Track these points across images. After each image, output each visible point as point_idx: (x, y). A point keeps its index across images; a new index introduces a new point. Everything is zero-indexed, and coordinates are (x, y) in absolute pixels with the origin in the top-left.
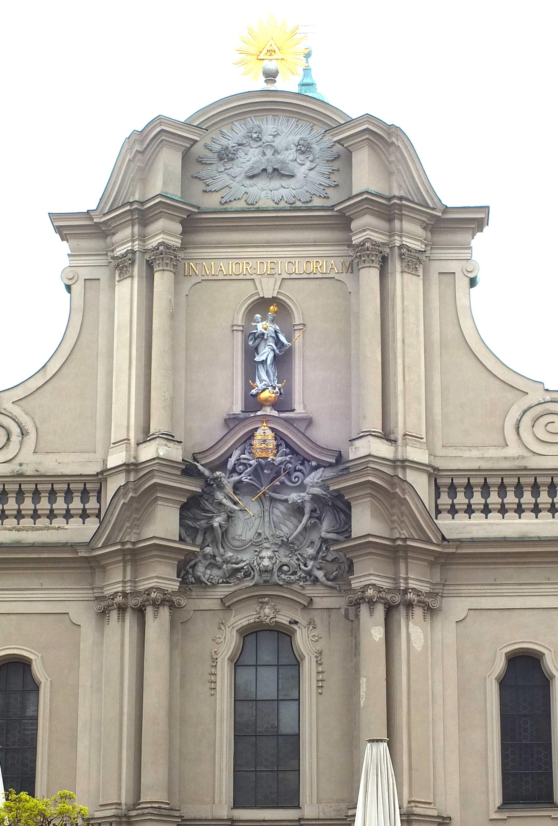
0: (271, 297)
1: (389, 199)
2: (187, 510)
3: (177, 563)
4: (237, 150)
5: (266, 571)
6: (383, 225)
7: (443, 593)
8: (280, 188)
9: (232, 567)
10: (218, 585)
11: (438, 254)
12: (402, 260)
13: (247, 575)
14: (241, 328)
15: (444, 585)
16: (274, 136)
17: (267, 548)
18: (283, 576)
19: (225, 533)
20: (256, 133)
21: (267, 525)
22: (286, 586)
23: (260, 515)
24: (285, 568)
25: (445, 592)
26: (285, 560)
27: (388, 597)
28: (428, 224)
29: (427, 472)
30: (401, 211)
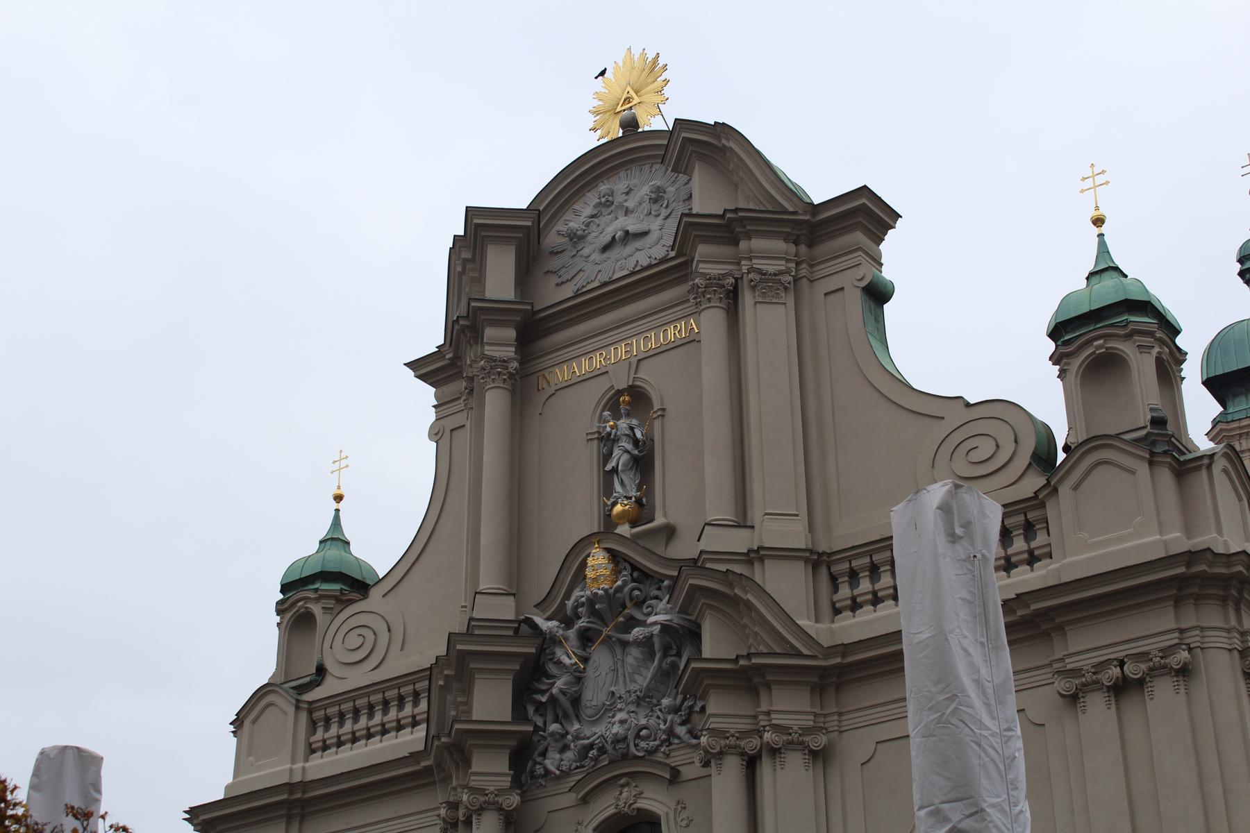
0: (626, 387)
1: (722, 216)
2: (537, 682)
3: (508, 751)
4: (588, 225)
5: (618, 740)
6: (724, 251)
7: (840, 727)
8: (635, 252)
9: (582, 745)
10: (572, 772)
11: (822, 270)
12: (753, 288)
13: (602, 751)
14: (596, 436)
15: (840, 714)
16: (627, 193)
17: (621, 710)
18: (643, 744)
19: (576, 701)
20: (604, 197)
21: (621, 679)
22: (647, 758)
23: (613, 668)
24: (644, 733)
25: (844, 723)
26: (643, 722)
27: (742, 743)
28: (798, 236)
29: (806, 561)
30: (744, 227)
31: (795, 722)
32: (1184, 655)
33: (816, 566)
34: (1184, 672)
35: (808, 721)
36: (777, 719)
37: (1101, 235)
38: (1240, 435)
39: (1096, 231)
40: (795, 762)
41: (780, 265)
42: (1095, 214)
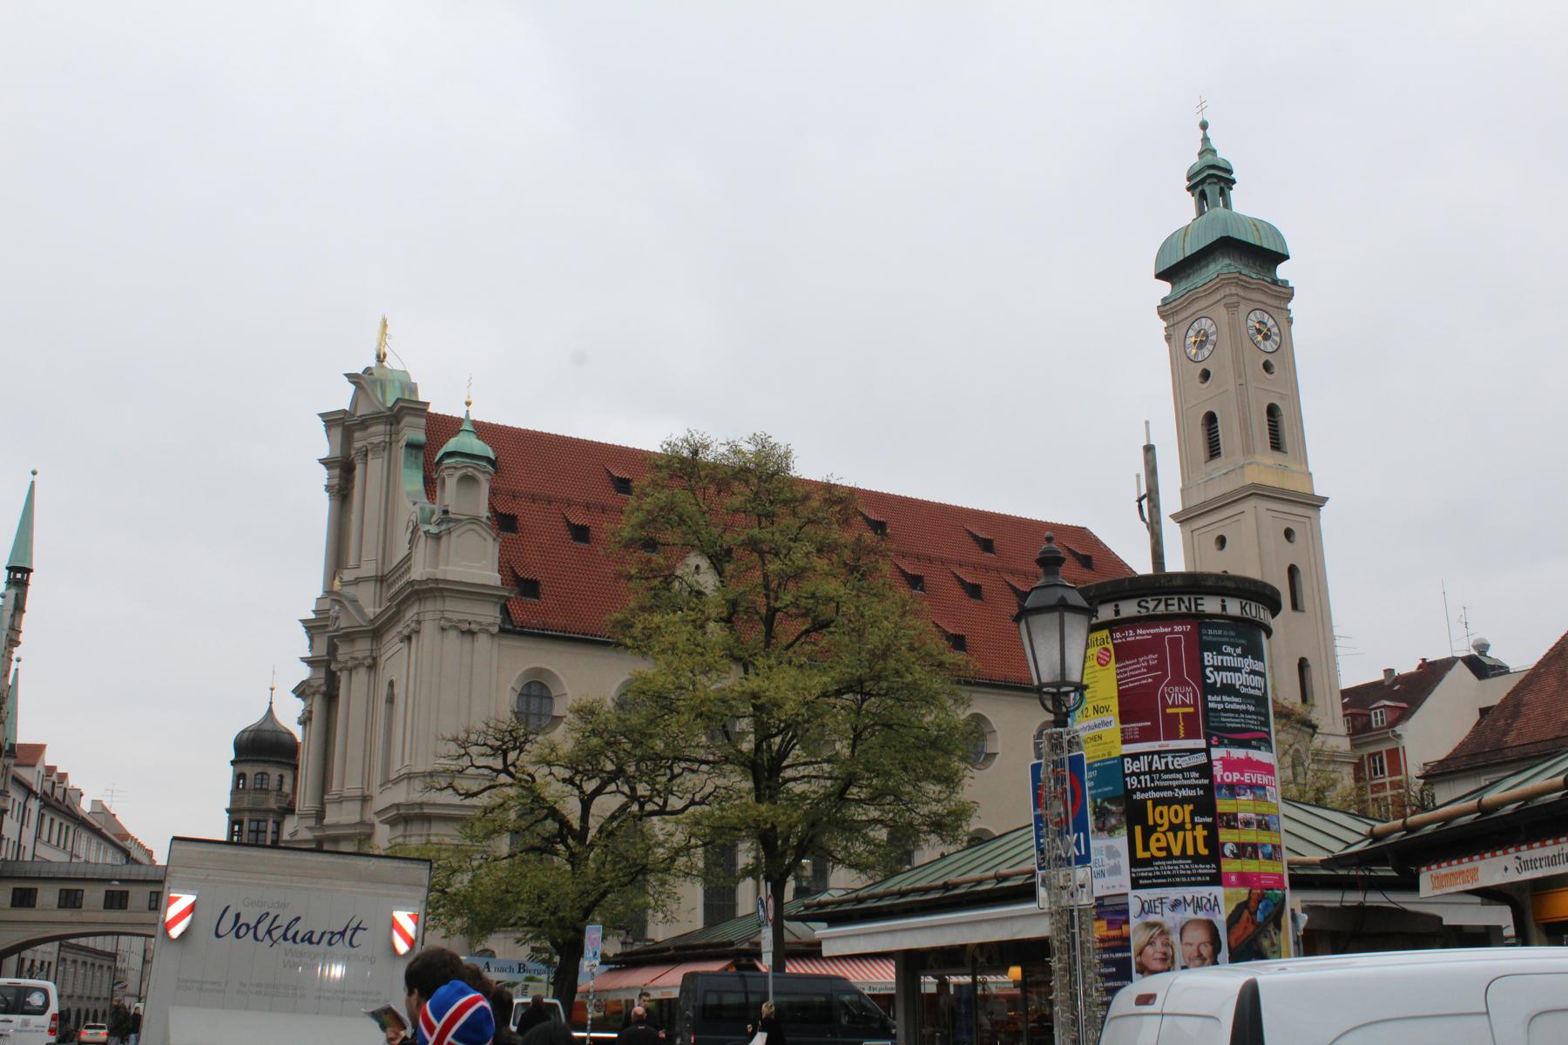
11: (401, 435)
29: (376, 581)
31: (360, 655)
32: (413, 625)
33: (382, 582)
34: (418, 632)
35: (368, 653)
36: (356, 655)
37: (468, 411)
38: (1173, 313)
39: (466, 408)
40: (362, 671)
41: (381, 438)
42: (467, 400)
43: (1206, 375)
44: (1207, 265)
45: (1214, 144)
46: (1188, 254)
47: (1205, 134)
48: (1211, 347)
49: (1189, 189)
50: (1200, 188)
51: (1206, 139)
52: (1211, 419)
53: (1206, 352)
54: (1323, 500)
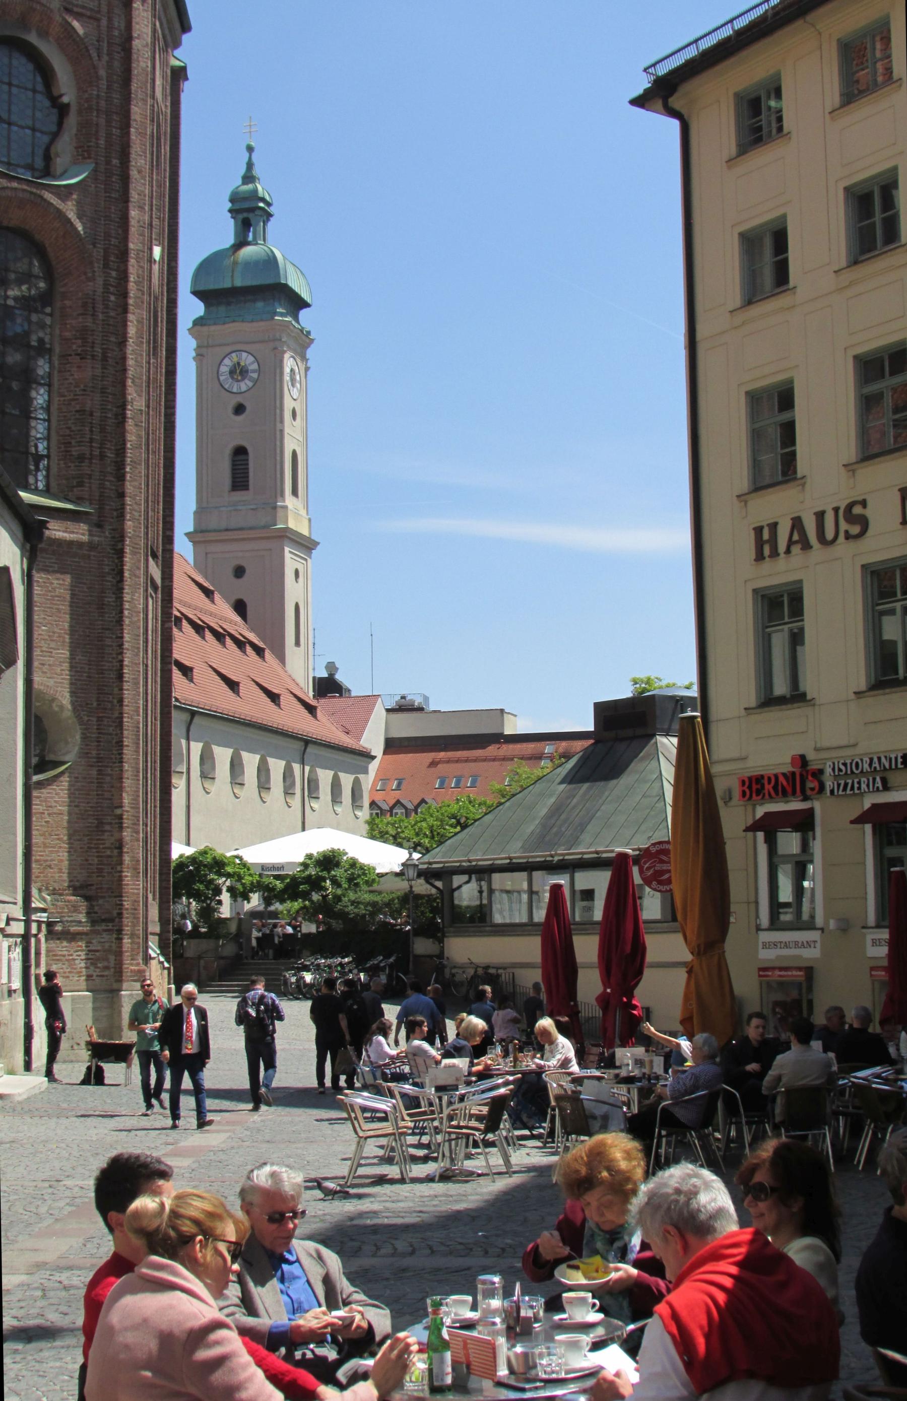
43: (239, 409)
44: (254, 301)
45: (257, 171)
46: (238, 283)
47: (250, 158)
48: (250, 384)
49: (230, 211)
50: (245, 215)
51: (250, 165)
52: (240, 452)
53: (244, 386)
54: (318, 543)
